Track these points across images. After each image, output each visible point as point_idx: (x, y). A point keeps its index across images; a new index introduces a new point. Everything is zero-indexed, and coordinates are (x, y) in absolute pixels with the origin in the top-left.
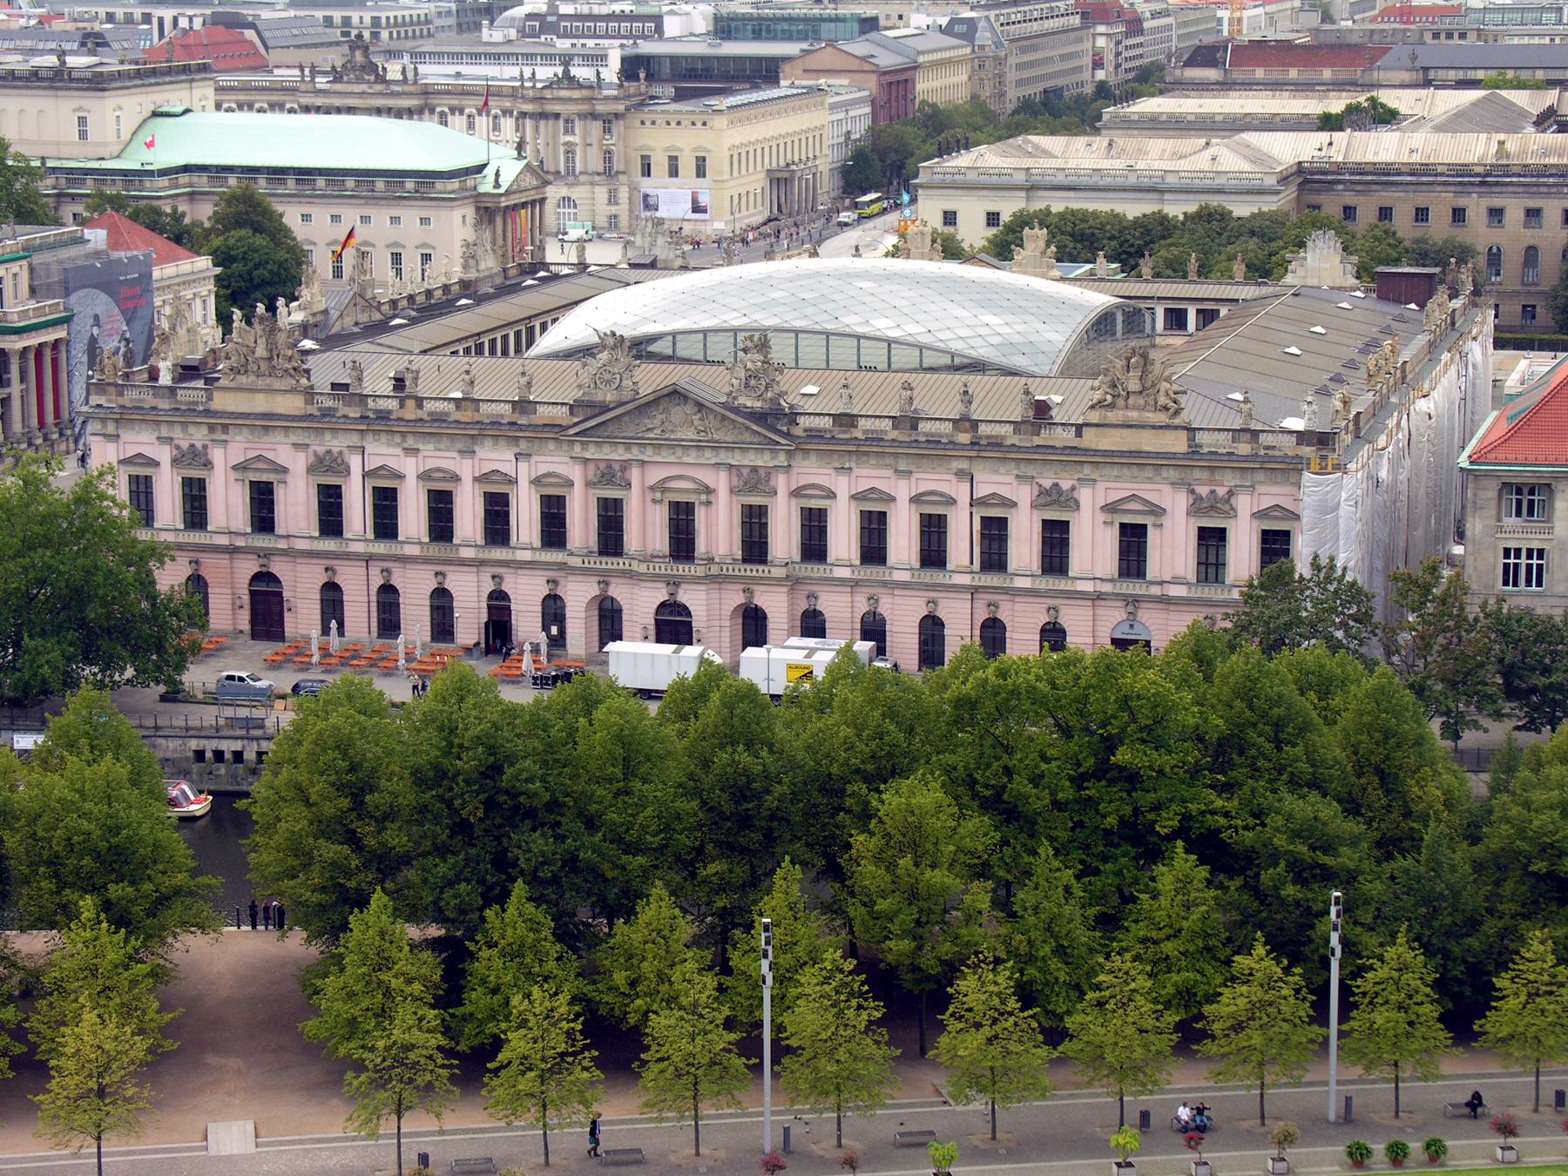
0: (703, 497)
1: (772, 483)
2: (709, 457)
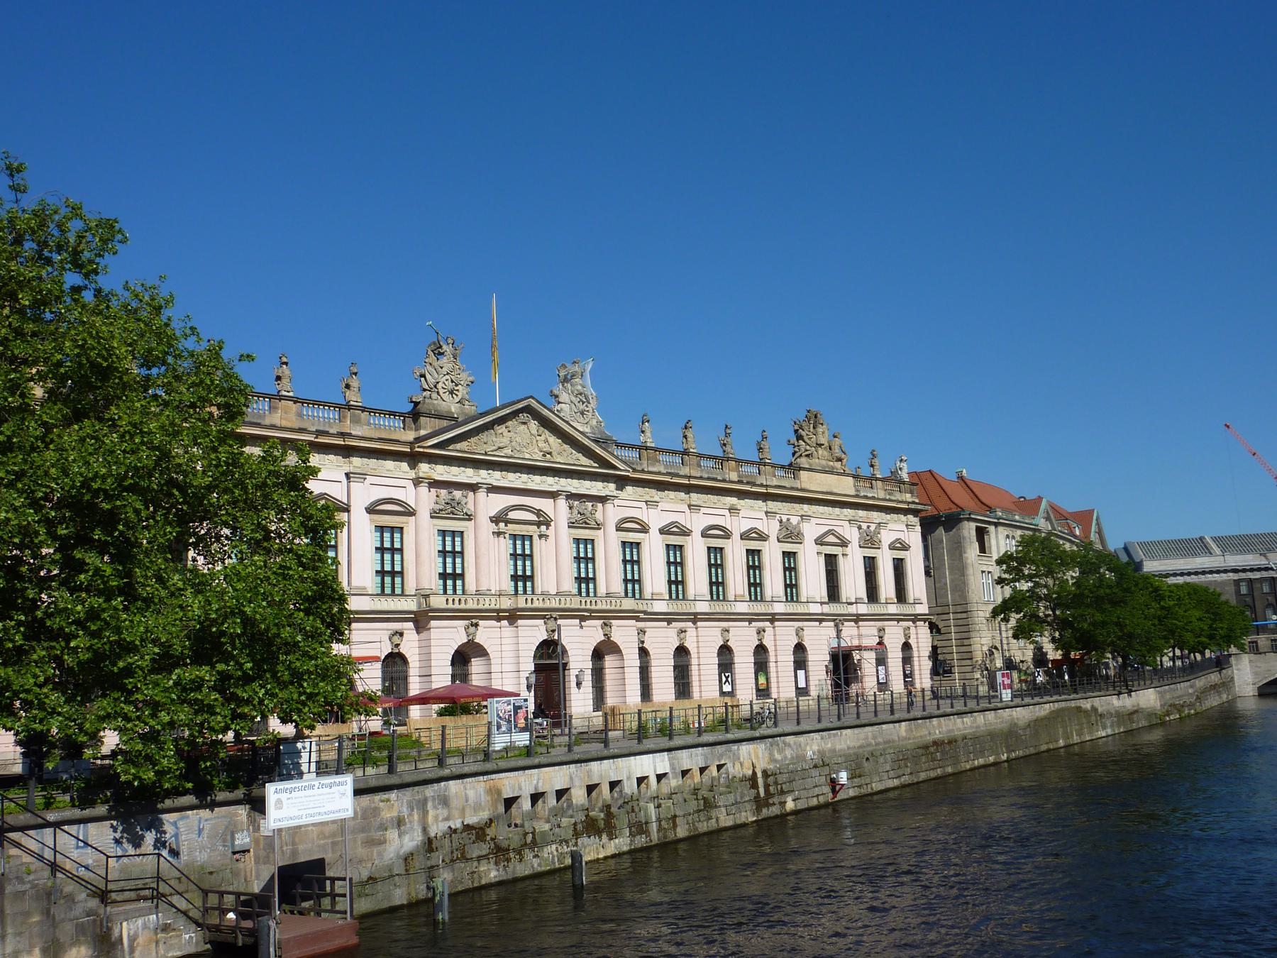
0: (543, 528)
1: (599, 516)
2: (549, 483)
